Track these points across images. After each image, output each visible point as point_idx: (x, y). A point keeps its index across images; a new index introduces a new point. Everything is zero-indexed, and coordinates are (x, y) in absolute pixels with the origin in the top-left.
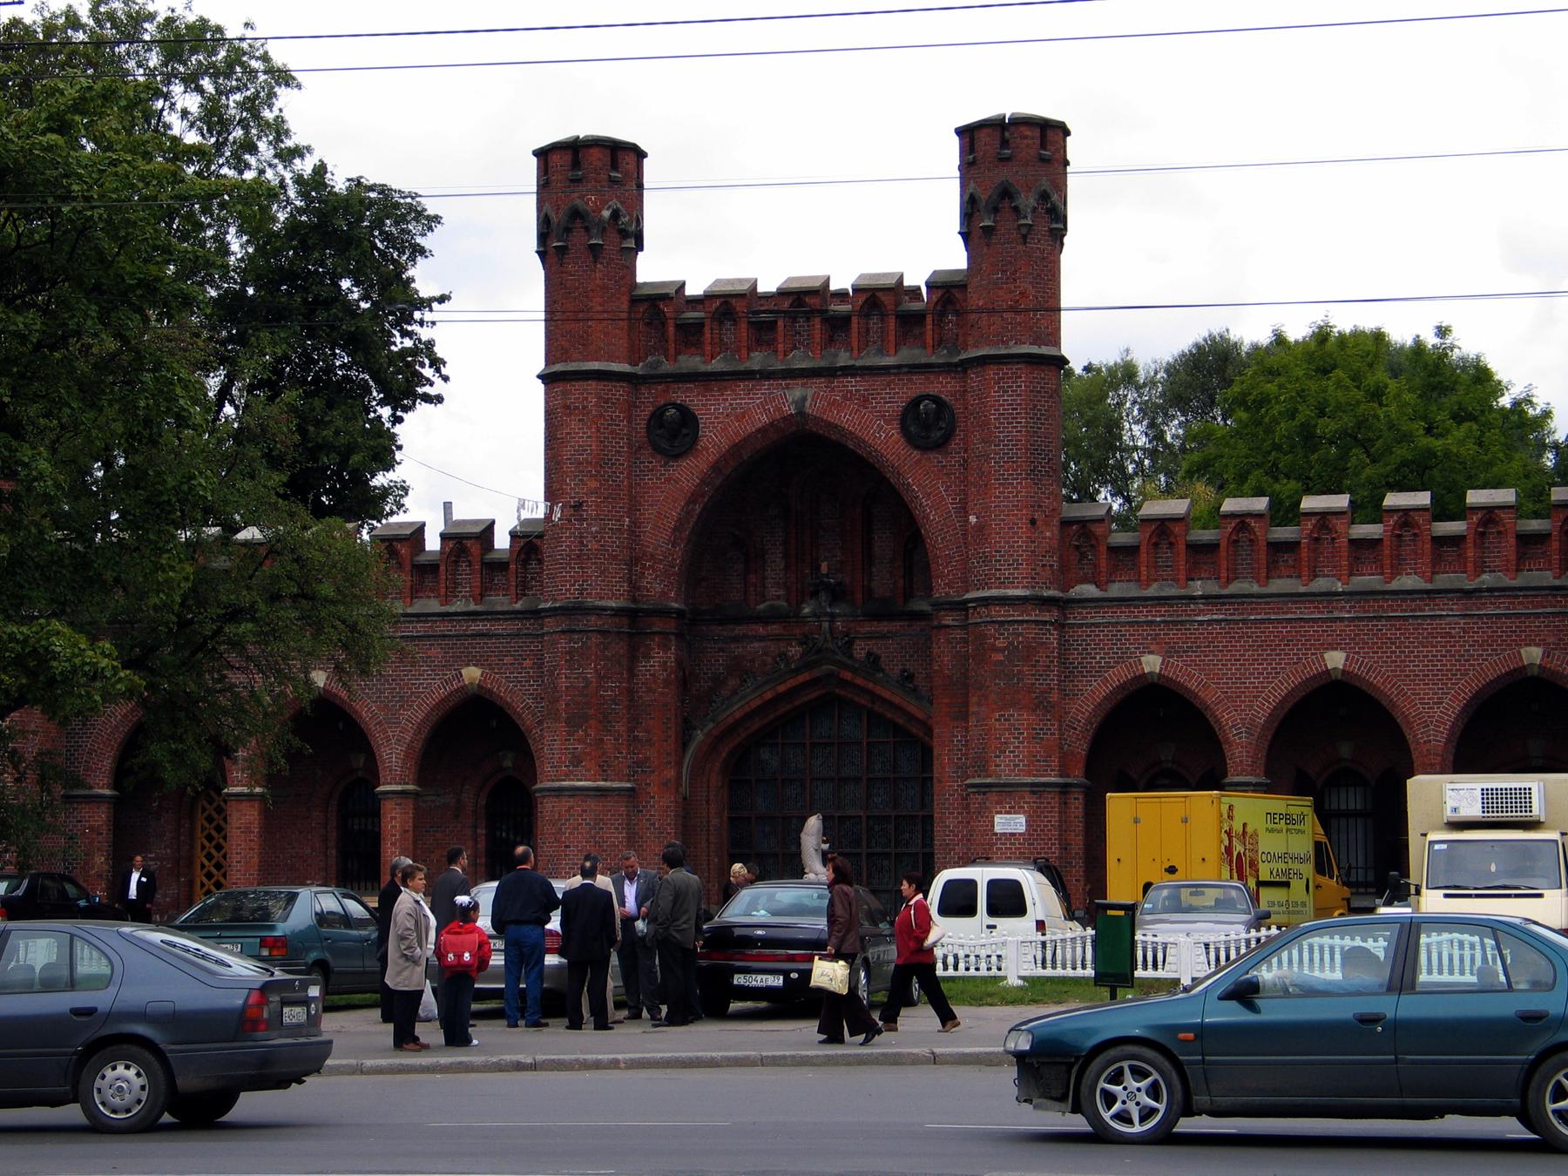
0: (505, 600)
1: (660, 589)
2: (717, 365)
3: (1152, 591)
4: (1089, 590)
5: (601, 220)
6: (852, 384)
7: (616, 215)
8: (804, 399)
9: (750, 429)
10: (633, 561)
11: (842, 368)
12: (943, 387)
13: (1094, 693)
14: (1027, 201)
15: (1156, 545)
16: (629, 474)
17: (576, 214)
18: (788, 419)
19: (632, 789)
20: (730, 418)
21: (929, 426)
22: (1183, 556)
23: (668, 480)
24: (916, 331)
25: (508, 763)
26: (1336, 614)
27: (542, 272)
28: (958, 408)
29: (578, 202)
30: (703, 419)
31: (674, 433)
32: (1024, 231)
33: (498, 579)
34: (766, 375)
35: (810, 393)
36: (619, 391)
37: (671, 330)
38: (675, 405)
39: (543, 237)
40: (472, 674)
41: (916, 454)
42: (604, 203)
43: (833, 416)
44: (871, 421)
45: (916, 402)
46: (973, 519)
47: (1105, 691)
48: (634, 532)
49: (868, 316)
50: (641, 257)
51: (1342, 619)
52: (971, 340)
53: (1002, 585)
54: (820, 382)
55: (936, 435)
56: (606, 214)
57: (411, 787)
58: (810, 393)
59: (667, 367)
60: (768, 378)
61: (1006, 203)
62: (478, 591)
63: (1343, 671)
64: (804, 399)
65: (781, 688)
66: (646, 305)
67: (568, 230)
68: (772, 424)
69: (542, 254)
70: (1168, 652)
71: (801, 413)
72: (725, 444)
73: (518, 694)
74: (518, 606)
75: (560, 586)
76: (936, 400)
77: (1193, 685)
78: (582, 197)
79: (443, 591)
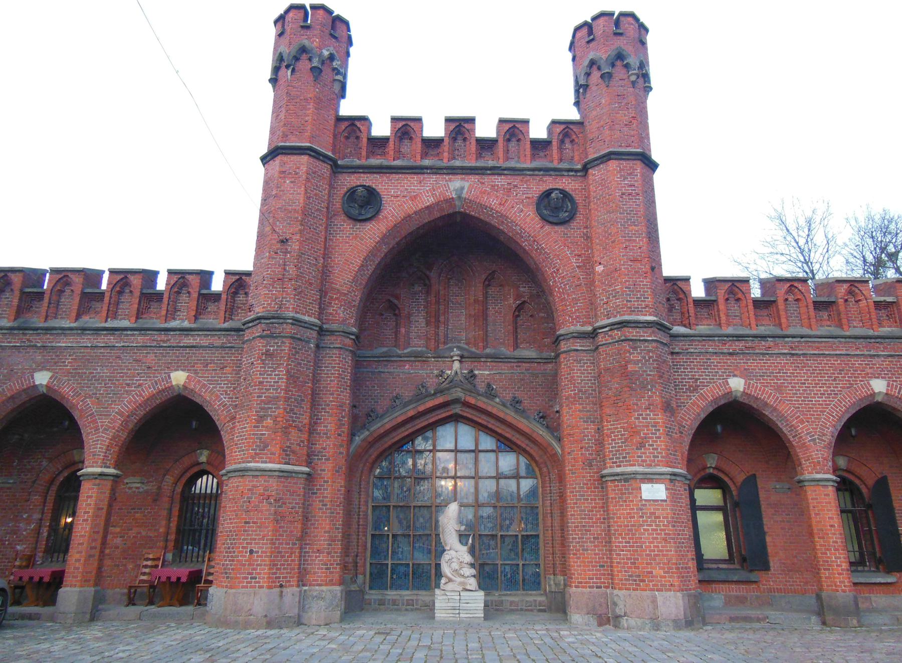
0: (214, 321)
1: (342, 315)
2: (398, 163)
3: (730, 330)
4: (681, 330)
5: (320, 55)
6: (500, 181)
7: (331, 58)
8: (462, 188)
9: (420, 206)
10: (323, 293)
11: (492, 168)
12: (569, 184)
13: (695, 408)
14: (633, 61)
15: (727, 299)
16: (326, 228)
17: (303, 50)
19: (309, 474)
21: (556, 208)
22: (751, 307)
23: (355, 238)
24: (542, 154)
25: (203, 459)
26: (872, 353)
27: (272, 94)
28: (578, 198)
29: (306, 43)
30: (385, 199)
31: (364, 204)
32: (633, 78)
33: (211, 307)
34: (436, 170)
35: (466, 185)
36: (325, 169)
37: (365, 140)
38: (364, 186)
39: (276, 70)
40: (179, 378)
41: (548, 228)
42: (326, 46)
43: (485, 200)
44: (511, 205)
45: (547, 194)
46: (599, 269)
47: (702, 404)
48: (325, 273)
49: (509, 140)
50: (343, 102)
51: (878, 356)
52: (591, 150)
53: (632, 312)
54: (474, 179)
55: (564, 215)
56: (326, 53)
57: (112, 471)
58: (466, 185)
59: (357, 162)
60: (436, 173)
61: (619, 63)
62: (193, 313)
63: (887, 394)
64: (462, 188)
65: (421, 408)
66: (347, 123)
67: (297, 59)
68: (437, 204)
69: (274, 81)
71: (459, 197)
73: (216, 398)
74: (226, 325)
75: (260, 302)
76: (562, 191)
77: (771, 401)
78: (309, 38)
79: (164, 313)
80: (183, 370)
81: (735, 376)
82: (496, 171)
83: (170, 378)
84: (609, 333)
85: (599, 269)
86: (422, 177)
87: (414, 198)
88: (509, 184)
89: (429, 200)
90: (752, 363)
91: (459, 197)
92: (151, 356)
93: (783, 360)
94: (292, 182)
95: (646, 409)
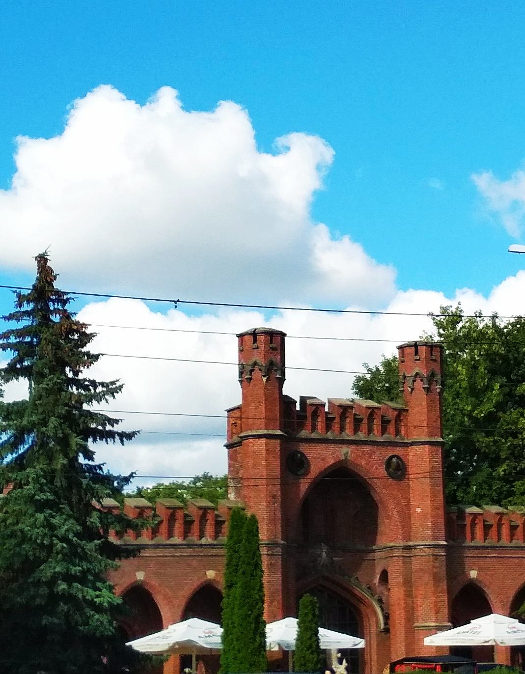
6: (366, 448)
18: (340, 462)
20: (320, 458)
34: (334, 442)
35: (349, 450)
43: (359, 461)
54: (353, 447)
58: (349, 450)
68: (334, 464)
70: (480, 570)
72: (318, 471)
76: (398, 458)
80: (212, 570)
81: (473, 570)
82: (365, 443)
83: (206, 575)
84: (424, 549)
85: (419, 510)
86: (327, 445)
87: (323, 459)
88: (371, 450)
89: (331, 461)
90: (481, 562)
91: (346, 459)
92: (195, 562)
93: (494, 560)
94: (273, 457)
95: (440, 593)
